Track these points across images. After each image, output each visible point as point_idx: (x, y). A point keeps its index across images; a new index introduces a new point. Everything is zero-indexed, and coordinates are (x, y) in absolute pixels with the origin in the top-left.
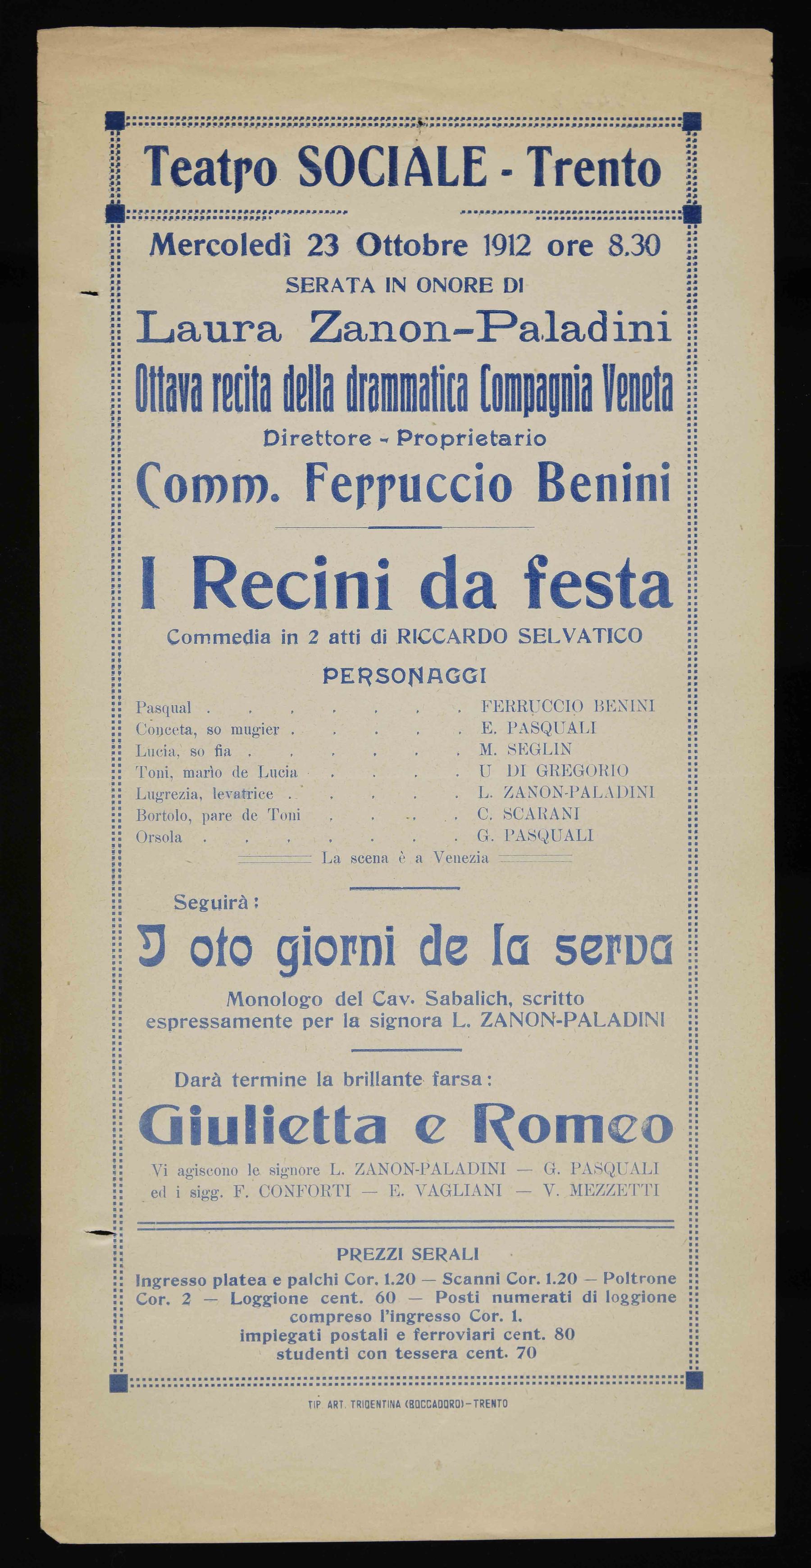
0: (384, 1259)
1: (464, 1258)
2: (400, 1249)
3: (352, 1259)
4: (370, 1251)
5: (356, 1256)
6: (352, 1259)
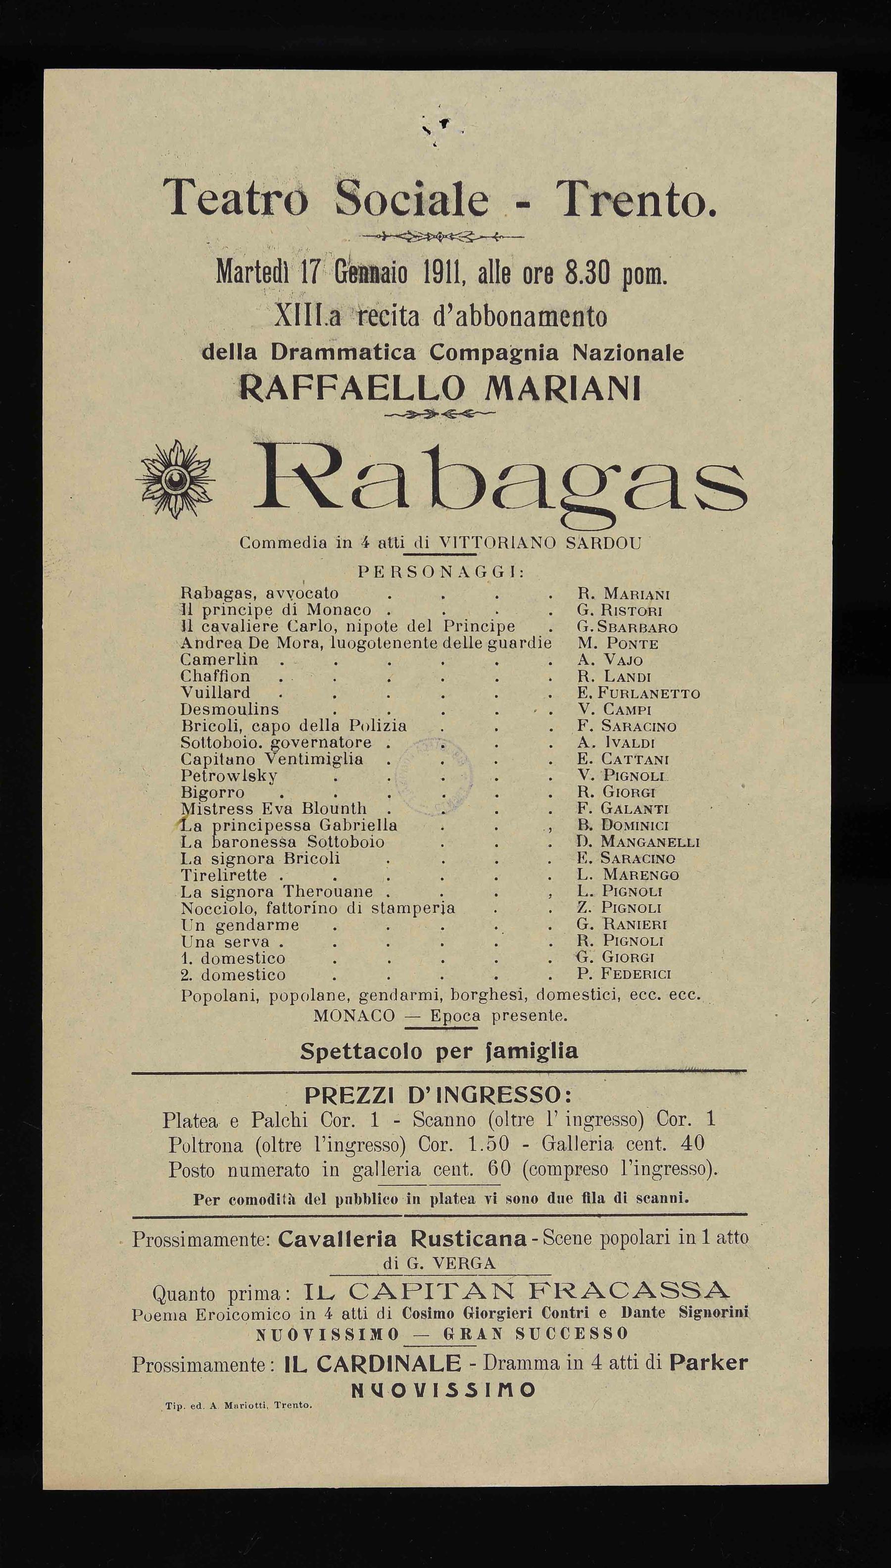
0: (368, 1102)
2: (391, 1089)
4: (350, 1091)
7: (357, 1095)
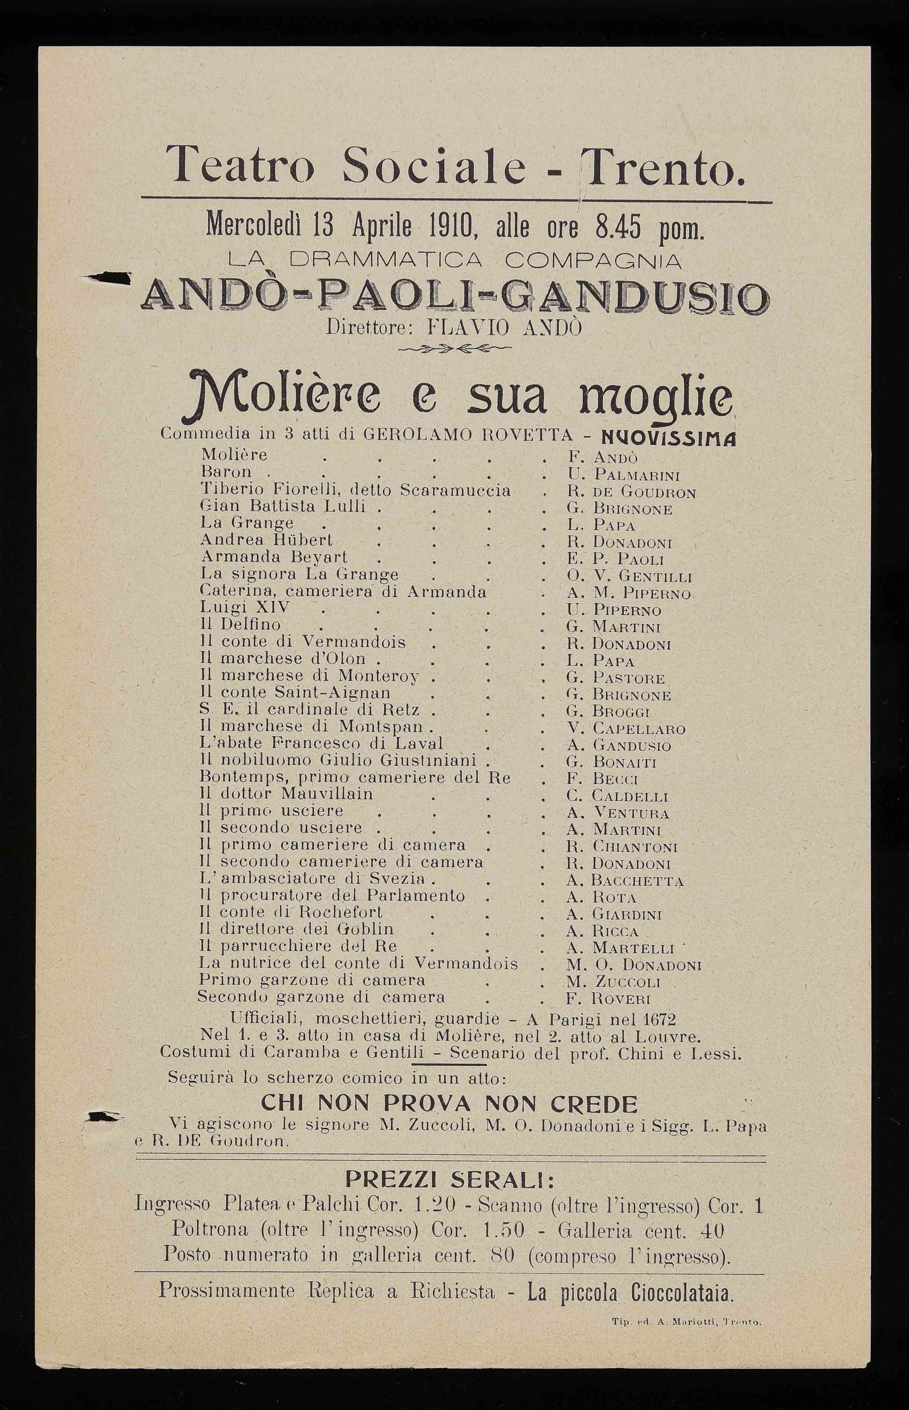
0: (410, 1186)
1: (523, 1186)
2: (434, 1173)
3: (366, 1185)
4: (392, 1175)
5: (371, 1182)
6: (366, 1185)
7: (399, 1178)
